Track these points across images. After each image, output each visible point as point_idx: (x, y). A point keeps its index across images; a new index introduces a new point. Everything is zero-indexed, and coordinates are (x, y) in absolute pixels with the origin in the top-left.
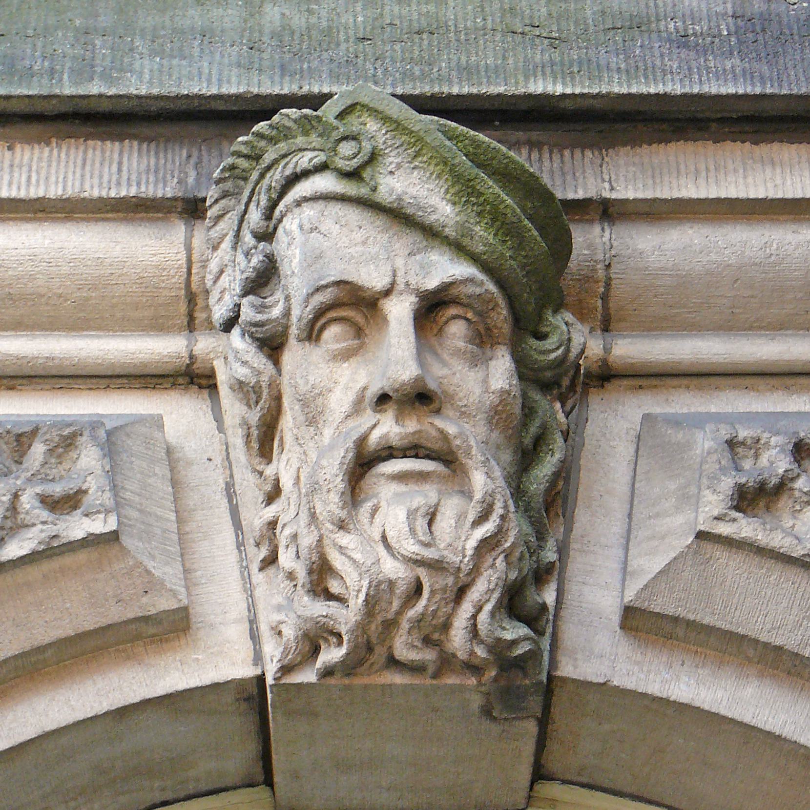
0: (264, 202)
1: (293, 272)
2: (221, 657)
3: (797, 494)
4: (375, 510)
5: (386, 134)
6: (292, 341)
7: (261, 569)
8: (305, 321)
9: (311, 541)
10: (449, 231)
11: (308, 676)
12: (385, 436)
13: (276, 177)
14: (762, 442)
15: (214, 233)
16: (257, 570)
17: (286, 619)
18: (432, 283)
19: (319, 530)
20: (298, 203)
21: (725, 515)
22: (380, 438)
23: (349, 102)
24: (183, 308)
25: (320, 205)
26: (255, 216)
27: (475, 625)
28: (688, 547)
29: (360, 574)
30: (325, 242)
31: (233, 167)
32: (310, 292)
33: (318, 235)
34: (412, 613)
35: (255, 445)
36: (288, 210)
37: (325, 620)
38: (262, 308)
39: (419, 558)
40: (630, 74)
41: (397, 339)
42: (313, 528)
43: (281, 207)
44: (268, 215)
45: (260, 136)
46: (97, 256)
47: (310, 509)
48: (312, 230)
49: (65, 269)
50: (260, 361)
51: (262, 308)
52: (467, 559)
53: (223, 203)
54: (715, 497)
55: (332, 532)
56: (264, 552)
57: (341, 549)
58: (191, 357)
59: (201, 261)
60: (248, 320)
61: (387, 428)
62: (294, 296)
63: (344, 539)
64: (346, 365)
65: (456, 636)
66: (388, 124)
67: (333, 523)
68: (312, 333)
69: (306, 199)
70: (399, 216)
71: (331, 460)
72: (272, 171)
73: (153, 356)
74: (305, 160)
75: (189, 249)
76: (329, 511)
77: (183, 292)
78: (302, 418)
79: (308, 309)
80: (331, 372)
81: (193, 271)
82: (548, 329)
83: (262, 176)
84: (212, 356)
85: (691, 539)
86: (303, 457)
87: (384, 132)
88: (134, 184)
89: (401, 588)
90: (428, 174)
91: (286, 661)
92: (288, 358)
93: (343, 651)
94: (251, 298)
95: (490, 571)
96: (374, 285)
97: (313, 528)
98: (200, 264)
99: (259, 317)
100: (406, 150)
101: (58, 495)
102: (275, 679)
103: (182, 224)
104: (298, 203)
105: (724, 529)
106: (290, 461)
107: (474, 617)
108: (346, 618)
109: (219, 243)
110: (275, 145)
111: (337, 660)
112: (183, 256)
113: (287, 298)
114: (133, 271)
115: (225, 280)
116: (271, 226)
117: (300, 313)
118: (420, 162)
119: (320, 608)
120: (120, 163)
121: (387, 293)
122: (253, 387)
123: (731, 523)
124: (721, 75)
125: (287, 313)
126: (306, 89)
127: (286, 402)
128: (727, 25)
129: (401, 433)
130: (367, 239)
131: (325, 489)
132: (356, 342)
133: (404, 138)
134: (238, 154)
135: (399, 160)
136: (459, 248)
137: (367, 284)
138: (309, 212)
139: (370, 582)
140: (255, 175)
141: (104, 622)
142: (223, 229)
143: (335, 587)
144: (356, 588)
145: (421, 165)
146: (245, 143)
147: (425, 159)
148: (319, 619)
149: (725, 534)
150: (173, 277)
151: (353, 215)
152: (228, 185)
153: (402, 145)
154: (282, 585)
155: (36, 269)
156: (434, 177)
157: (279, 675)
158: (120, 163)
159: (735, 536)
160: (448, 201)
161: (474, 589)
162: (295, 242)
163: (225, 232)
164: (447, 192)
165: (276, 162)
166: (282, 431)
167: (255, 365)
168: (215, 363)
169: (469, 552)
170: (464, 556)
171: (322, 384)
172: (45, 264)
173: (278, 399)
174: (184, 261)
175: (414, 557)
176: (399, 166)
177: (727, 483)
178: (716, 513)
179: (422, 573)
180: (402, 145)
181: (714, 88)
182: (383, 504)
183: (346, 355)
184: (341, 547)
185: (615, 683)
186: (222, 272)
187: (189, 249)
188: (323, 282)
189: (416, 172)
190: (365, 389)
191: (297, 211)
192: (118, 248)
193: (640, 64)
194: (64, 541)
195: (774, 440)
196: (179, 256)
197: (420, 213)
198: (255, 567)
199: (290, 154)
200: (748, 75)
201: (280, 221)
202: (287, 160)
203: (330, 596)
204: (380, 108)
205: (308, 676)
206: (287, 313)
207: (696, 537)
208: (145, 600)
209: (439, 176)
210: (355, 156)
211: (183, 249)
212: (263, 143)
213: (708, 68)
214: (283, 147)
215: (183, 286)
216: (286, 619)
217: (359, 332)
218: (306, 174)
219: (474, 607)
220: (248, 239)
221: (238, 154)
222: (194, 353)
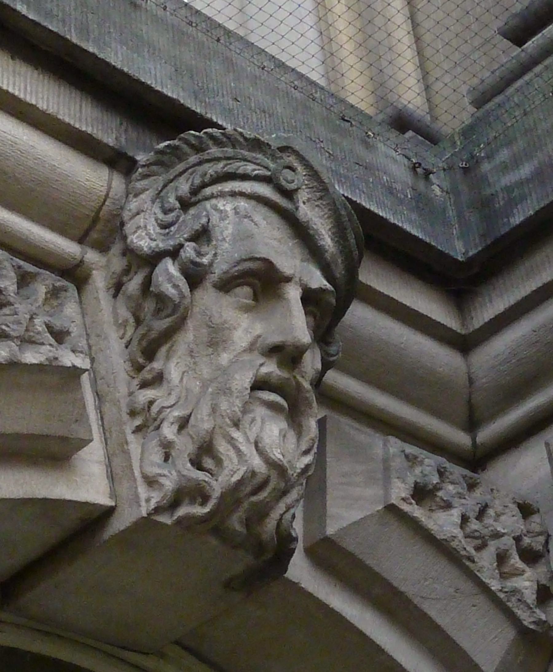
0: (198, 181)
1: (224, 239)
2: (87, 483)
3: (438, 499)
4: (253, 420)
5: (305, 175)
6: (208, 284)
7: (133, 432)
8: (229, 275)
9: (209, 427)
10: (328, 256)
11: (166, 519)
12: (269, 374)
13: (211, 169)
14: (419, 459)
15: (140, 185)
16: (130, 432)
17: (169, 474)
18: (314, 285)
19: (215, 421)
20: (234, 194)
21: (408, 499)
22: (266, 373)
23: (285, 144)
24: (86, 226)
25: (253, 203)
26: (184, 187)
27: (281, 519)
28: (378, 511)
29: (239, 461)
30: (241, 226)
31: (176, 148)
32: (244, 257)
33: (251, 222)
34: (254, 499)
35: (144, 343)
36: (222, 195)
37: (205, 484)
38: (199, 254)
39: (281, 463)
40: (370, 198)
41: (298, 313)
42: (211, 418)
43: (208, 191)
44: (195, 191)
45: (211, 137)
46: (53, 163)
47: (212, 404)
48: (246, 217)
49: (30, 163)
50: (185, 288)
51: (199, 254)
52: (295, 475)
53: (154, 168)
54: (403, 485)
55: (228, 425)
56: (138, 422)
57: (231, 441)
58: (82, 261)
59: (114, 199)
60: (192, 258)
61: (270, 368)
62: (222, 256)
63: (236, 434)
64: (246, 315)
65: (269, 523)
66: (308, 170)
67: (231, 420)
68: (226, 285)
69: (242, 194)
70: (301, 232)
71: (243, 377)
72: (212, 164)
73: (58, 250)
74: (249, 168)
75: (109, 187)
76: (234, 411)
77: (94, 214)
78: (205, 339)
79: (236, 269)
80: (237, 316)
81: (106, 203)
82: (331, 340)
83: (200, 163)
84: (94, 266)
85: (380, 507)
86: (192, 365)
87: (304, 173)
88: (90, 125)
89: (258, 480)
90: (323, 213)
91: (162, 504)
92: (199, 293)
93: (206, 510)
94: (193, 244)
95: (300, 487)
96: (284, 270)
97: (211, 418)
98: (112, 201)
99: (198, 260)
100: (314, 192)
101: (58, 328)
102: (148, 514)
103: (107, 169)
104: (234, 194)
105: (405, 507)
106: (179, 365)
107: (282, 515)
108: (217, 487)
109: (140, 193)
110: (221, 148)
111: (200, 514)
112: (104, 189)
113: (215, 255)
114: (71, 185)
115: (140, 220)
116: (193, 199)
117: (220, 268)
118: (321, 204)
119: (201, 475)
120: (81, 106)
121: (288, 279)
122: (175, 305)
123: (408, 505)
124: (410, 222)
125: (211, 264)
126: (209, 116)
127: (190, 324)
128: (410, 191)
129: (280, 375)
130: (282, 238)
131: (235, 395)
132: (253, 302)
133: (315, 184)
134: (187, 142)
135: (310, 196)
136: (327, 270)
137: (281, 270)
138: (243, 204)
139: (247, 469)
140: (193, 159)
141: (46, 431)
142: (146, 185)
143: (208, 463)
144: (234, 470)
145: (322, 206)
146: (194, 136)
147: (324, 203)
148: (201, 482)
149: (406, 511)
150: (93, 201)
151: (274, 218)
152: (165, 158)
153: (312, 188)
154: (156, 449)
155: (13, 154)
156: (326, 216)
157: (153, 512)
158: (81, 106)
159: (410, 514)
160: (329, 236)
161: (289, 495)
162: (228, 219)
163: (147, 187)
164: (330, 230)
165: (218, 159)
166: (175, 342)
167: (183, 291)
168: (94, 272)
169: (299, 471)
170: (295, 472)
171: (231, 322)
172: (19, 152)
173: (183, 319)
174: (104, 193)
175: (278, 461)
176: (309, 200)
177: (411, 480)
178: (403, 495)
179: (274, 475)
180: (312, 188)
181: (407, 227)
182: (259, 420)
183: (247, 309)
184: (232, 438)
185: (303, 586)
186: (138, 214)
187: (109, 187)
188: (258, 256)
189: (317, 209)
190: (259, 336)
191: (229, 198)
192: (67, 164)
193: (373, 194)
194: (60, 364)
195: (427, 461)
196: (102, 189)
197: (317, 237)
198: (128, 429)
199: (233, 159)
200: (423, 230)
201: (207, 199)
202: (229, 162)
203: (200, 468)
204: (307, 158)
205: (166, 519)
206: (211, 264)
207: (385, 507)
208: (73, 426)
209: (329, 218)
210: (293, 181)
211: (106, 185)
212: (210, 143)
213: (404, 214)
214: (229, 151)
215: (95, 210)
216: (169, 474)
217: (256, 298)
218: (245, 177)
219: (286, 507)
220: (172, 200)
221: (187, 142)
222: (84, 259)
